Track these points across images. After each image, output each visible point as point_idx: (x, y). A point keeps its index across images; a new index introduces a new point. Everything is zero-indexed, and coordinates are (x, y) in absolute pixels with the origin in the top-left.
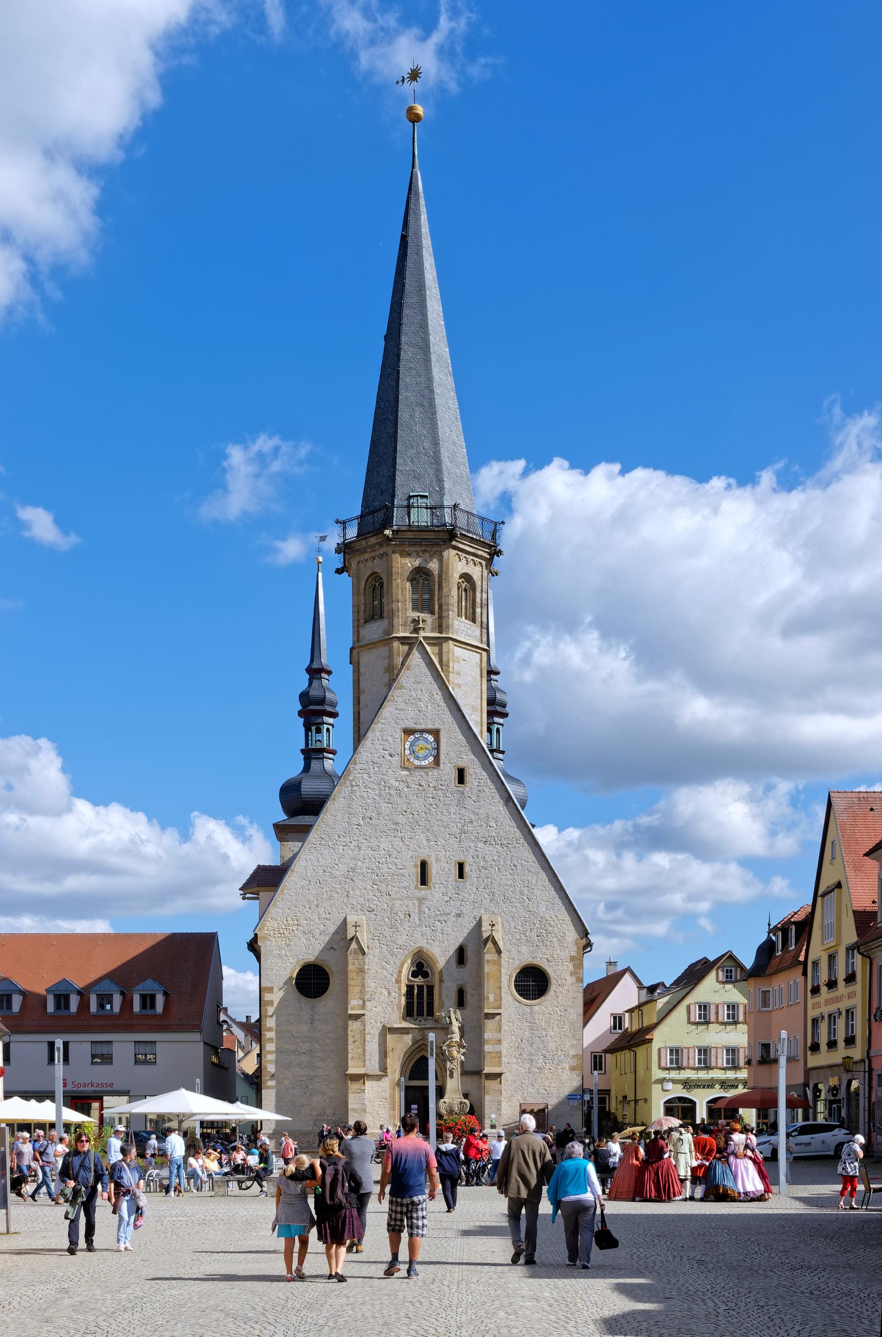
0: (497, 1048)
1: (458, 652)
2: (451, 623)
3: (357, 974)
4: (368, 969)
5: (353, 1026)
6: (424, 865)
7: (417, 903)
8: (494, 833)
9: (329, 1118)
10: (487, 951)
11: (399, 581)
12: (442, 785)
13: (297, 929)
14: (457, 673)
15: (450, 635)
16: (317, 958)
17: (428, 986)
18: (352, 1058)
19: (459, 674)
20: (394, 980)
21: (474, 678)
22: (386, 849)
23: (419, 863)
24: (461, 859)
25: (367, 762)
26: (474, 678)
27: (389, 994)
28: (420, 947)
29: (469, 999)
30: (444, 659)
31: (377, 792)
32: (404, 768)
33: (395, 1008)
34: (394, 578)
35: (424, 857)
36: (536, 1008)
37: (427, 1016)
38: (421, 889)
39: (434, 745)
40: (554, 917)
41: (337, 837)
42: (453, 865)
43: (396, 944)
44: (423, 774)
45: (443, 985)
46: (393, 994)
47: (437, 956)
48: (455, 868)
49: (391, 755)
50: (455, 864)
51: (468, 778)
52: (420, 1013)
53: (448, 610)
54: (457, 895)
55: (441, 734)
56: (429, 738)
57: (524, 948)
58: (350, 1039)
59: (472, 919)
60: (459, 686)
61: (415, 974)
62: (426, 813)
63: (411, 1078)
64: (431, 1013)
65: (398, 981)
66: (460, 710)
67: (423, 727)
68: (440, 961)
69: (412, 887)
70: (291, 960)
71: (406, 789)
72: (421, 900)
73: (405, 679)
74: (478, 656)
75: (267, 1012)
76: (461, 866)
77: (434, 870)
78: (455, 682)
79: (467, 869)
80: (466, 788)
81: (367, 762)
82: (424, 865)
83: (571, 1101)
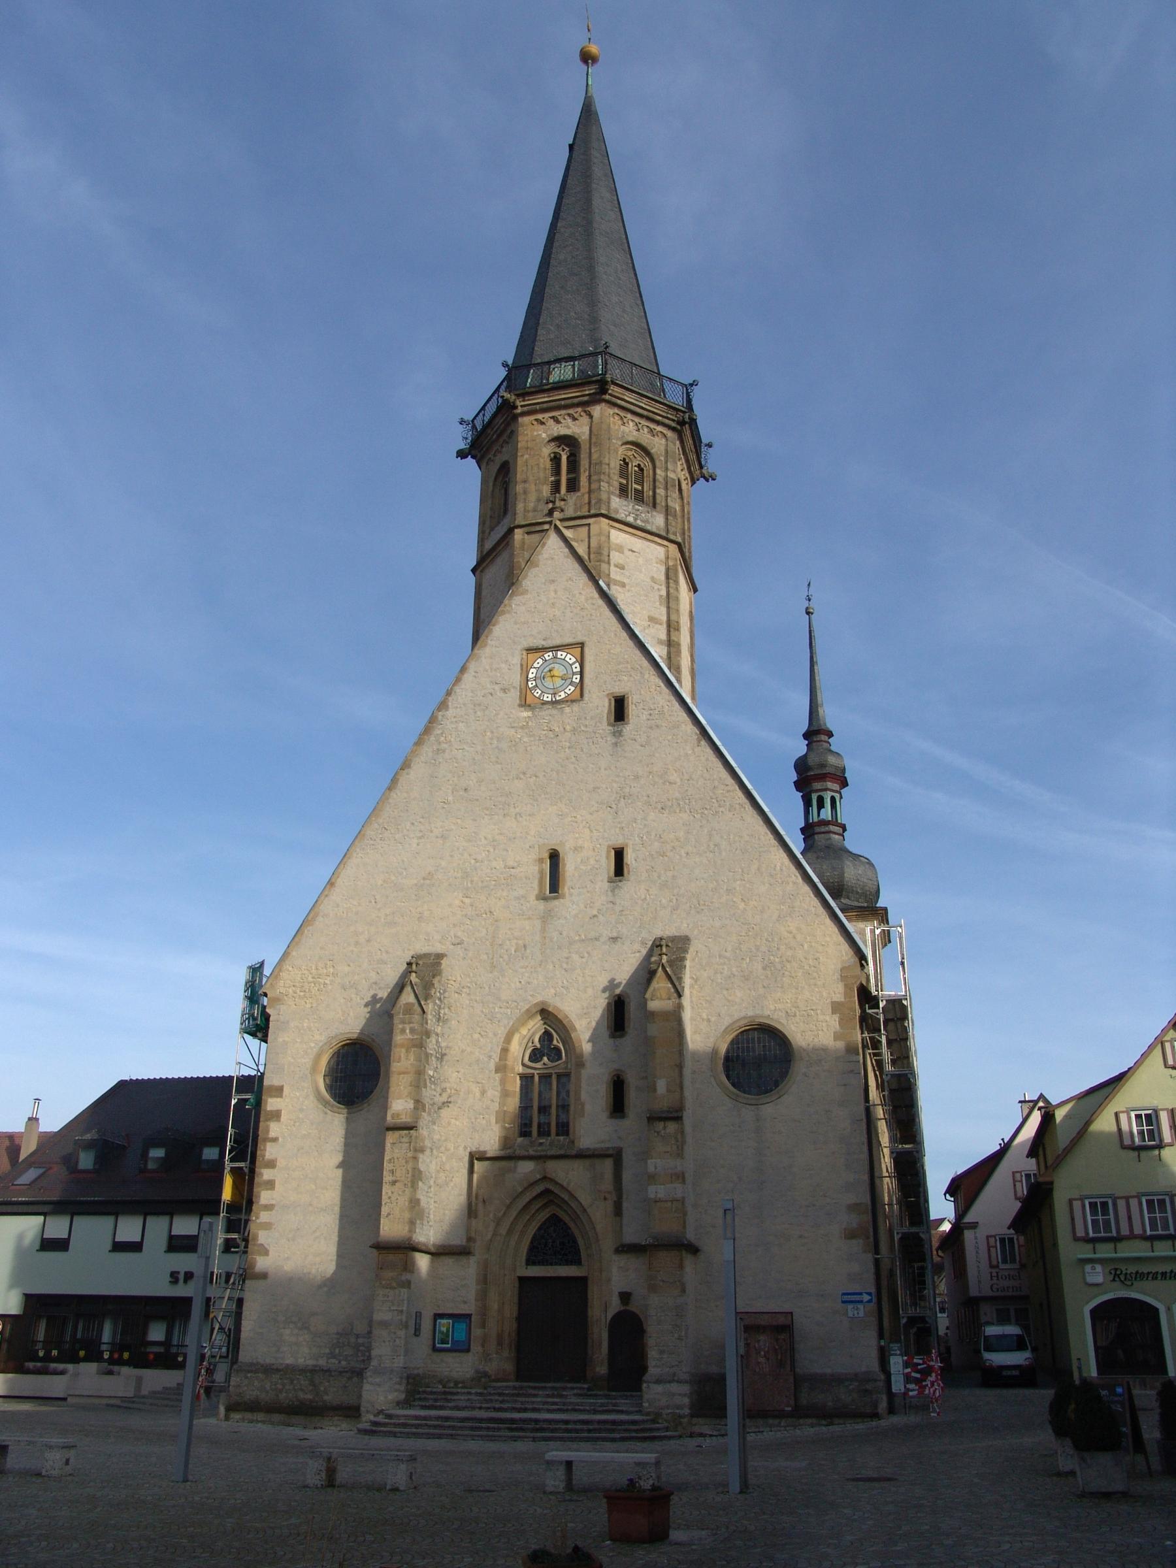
0: (678, 1190)
1: (618, 536)
2: (604, 496)
3: (407, 1051)
4: (447, 1047)
5: (394, 1148)
6: (554, 857)
7: (538, 923)
8: (677, 795)
9: (360, 1341)
10: (653, 995)
11: (526, 456)
12: (586, 726)
13: (332, 982)
14: (616, 566)
15: (603, 512)
16: (362, 1032)
17: (559, 1076)
18: (389, 1214)
19: (623, 568)
20: (492, 1066)
21: (653, 579)
22: (489, 836)
23: (546, 855)
24: (619, 843)
25: (464, 704)
26: (653, 579)
27: (483, 1092)
28: (543, 1003)
29: (633, 1098)
30: (594, 544)
31: (479, 748)
32: (524, 704)
33: (493, 1120)
34: (519, 454)
35: (553, 843)
36: (768, 1110)
37: (557, 1135)
38: (545, 899)
39: (576, 668)
40: (794, 931)
41: (408, 824)
42: (604, 854)
43: (499, 999)
44: (554, 712)
45: (583, 1071)
46: (490, 1093)
47: (573, 1017)
48: (607, 858)
49: (504, 690)
50: (608, 852)
51: (632, 710)
52: (544, 1131)
53: (599, 481)
54: (612, 905)
55: (586, 650)
56: (567, 659)
57: (739, 994)
58: (387, 1177)
59: (637, 946)
60: (623, 585)
61: (535, 1056)
62: (558, 772)
63: (530, 1262)
64: (564, 1129)
65: (501, 1068)
66: (629, 628)
67: (558, 642)
68: (577, 1026)
69: (532, 897)
70: (317, 1037)
71: (526, 739)
72: (546, 918)
73: (533, 580)
74: (661, 550)
75: (268, 1131)
76: (619, 855)
77: (570, 866)
78: (613, 576)
79: (629, 858)
80: (628, 729)
81: (464, 704)
82: (554, 857)
83: (850, 1306)
